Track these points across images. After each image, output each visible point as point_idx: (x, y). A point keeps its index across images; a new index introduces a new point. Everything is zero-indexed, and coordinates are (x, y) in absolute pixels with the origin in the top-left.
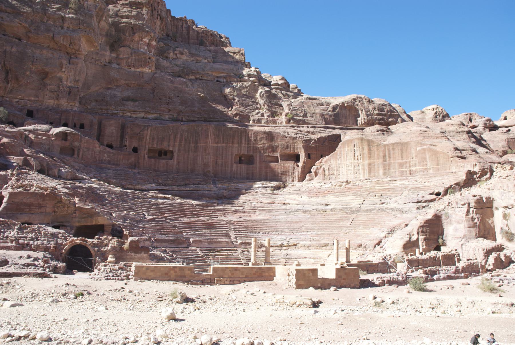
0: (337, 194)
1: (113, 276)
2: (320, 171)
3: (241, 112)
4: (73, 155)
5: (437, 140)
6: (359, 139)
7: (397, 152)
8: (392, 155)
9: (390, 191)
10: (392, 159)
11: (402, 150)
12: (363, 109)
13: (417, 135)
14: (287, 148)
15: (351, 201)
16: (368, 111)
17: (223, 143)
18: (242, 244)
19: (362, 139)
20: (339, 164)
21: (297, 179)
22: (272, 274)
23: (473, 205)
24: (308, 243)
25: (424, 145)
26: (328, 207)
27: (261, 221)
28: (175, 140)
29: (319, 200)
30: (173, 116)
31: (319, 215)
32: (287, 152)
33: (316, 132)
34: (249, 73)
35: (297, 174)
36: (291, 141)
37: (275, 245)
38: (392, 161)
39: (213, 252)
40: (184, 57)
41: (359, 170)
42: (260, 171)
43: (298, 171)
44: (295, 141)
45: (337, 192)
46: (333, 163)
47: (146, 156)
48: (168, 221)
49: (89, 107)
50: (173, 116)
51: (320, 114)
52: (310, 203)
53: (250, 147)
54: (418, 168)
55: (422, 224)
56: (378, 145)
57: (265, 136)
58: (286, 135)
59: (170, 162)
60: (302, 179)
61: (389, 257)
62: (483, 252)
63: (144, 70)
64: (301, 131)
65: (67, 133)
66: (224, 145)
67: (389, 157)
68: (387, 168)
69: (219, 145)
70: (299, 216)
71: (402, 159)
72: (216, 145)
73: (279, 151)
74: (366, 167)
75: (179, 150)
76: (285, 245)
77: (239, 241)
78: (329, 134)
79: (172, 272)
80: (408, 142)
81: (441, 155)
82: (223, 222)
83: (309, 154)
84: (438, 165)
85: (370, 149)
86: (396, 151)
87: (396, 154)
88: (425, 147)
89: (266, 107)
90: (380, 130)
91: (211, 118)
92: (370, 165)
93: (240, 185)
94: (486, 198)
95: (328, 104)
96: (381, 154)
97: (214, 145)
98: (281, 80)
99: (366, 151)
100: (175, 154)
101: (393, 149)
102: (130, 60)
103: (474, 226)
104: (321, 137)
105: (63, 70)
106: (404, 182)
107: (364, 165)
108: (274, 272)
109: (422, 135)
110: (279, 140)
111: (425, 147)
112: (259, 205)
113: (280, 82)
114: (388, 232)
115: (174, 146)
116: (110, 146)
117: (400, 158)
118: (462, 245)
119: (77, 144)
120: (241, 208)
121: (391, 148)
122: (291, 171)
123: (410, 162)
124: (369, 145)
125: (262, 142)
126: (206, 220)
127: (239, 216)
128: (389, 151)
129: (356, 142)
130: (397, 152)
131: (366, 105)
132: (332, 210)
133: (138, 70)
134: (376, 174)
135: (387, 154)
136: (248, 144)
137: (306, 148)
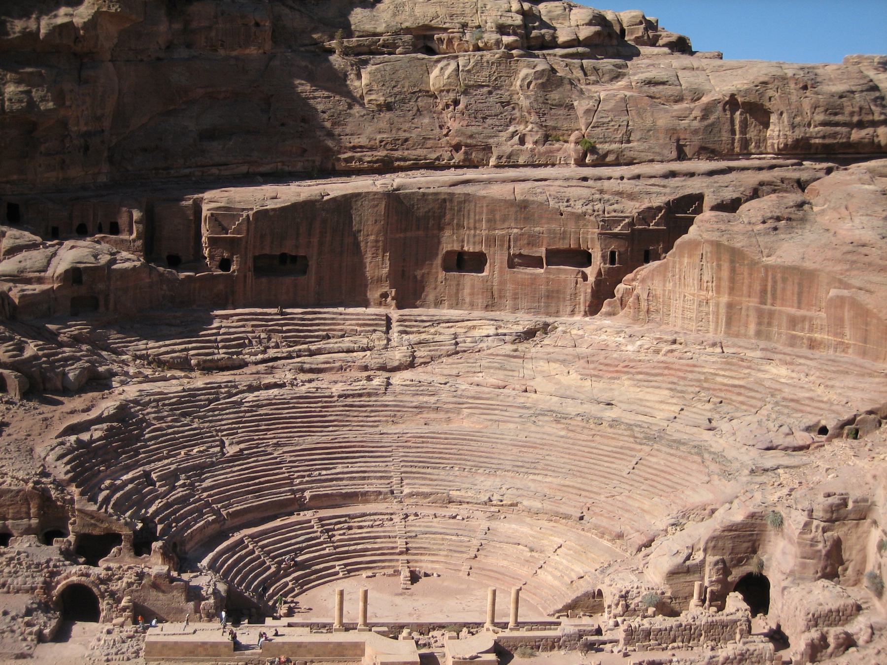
0: (640, 377)
1: (116, 654)
3: (471, 137)
4: (96, 307)
6: (712, 243)
7: (791, 289)
8: (779, 291)
9: (739, 394)
10: (778, 301)
11: (800, 285)
12: (783, 109)
13: (838, 254)
14: (564, 238)
15: (657, 406)
16: (799, 112)
17: (418, 229)
18: (411, 495)
19: (717, 245)
20: (670, 291)
21: (582, 308)
22: (359, 652)
23: (819, 513)
24: (536, 504)
25: (847, 286)
26: (610, 414)
30: (314, 161)
31: (586, 431)
32: (562, 245)
33: (640, 193)
34: (500, 22)
37: (475, 501)
39: (345, 522)
41: (708, 314)
42: (500, 291)
43: (586, 290)
44: (581, 223)
45: (641, 373)
46: (657, 286)
47: (250, 274)
48: (269, 450)
49: (130, 168)
50: (314, 161)
51: (667, 131)
52: (577, 395)
53: (479, 235)
54: (826, 337)
55: (717, 533)
56: (753, 264)
57: (513, 210)
58: (562, 206)
60: (593, 309)
61: (635, 591)
62: (804, 618)
63: (247, 51)
64: (601, 192)
65: (79, 268)
66: (421, 233)
68: (765, 320)
69: (409, 234)
70: (547, 429)
71: (799, 307)
72: (402, 235)
73: (545, 243)
74: (723, 311)
76: (494, 502)
77: (407, 490)
78: (671, 198)
79: (200, 649)
80: (816, 270)
81: (875, 321)
82: (386, 439)
83: (613, 254)
84: (865, 342)
85: (733, 270)
87: (789, 293)
88: (845, 293)
89: (533, 118)
90: (771, 218)
91: (398, 160)
92: (730, 306)
94: (855, 502)
96: (757, 287)
97: (398, 236)
98: (587, 24)
99: (725, 274)
100: (313, 264)
101: (784, 280)
102: (213, 34)
103: (815, 555)
105: (68, 103)
107: (717, 305)
108: (363, 651)
109: (849, 257)
110: (544, 221)
111: (845, 293)
113: (585, 32)
114: (673, 521)
117: (796, 305)
118: (784, 588)
119: (101, 286)
120: (433, 399)
121: (779, 275)
122: (569, 292)
123: (811, 319)
124: (732, 262)
125: (506, 225)
126: (351, 436)
127: (423, 421)
128: (775, 282)
129: (706, 249)
131: (794, 98)
132: (614, 423)
134: (743, 331)
135: (769, 288)
136: (475, 228)
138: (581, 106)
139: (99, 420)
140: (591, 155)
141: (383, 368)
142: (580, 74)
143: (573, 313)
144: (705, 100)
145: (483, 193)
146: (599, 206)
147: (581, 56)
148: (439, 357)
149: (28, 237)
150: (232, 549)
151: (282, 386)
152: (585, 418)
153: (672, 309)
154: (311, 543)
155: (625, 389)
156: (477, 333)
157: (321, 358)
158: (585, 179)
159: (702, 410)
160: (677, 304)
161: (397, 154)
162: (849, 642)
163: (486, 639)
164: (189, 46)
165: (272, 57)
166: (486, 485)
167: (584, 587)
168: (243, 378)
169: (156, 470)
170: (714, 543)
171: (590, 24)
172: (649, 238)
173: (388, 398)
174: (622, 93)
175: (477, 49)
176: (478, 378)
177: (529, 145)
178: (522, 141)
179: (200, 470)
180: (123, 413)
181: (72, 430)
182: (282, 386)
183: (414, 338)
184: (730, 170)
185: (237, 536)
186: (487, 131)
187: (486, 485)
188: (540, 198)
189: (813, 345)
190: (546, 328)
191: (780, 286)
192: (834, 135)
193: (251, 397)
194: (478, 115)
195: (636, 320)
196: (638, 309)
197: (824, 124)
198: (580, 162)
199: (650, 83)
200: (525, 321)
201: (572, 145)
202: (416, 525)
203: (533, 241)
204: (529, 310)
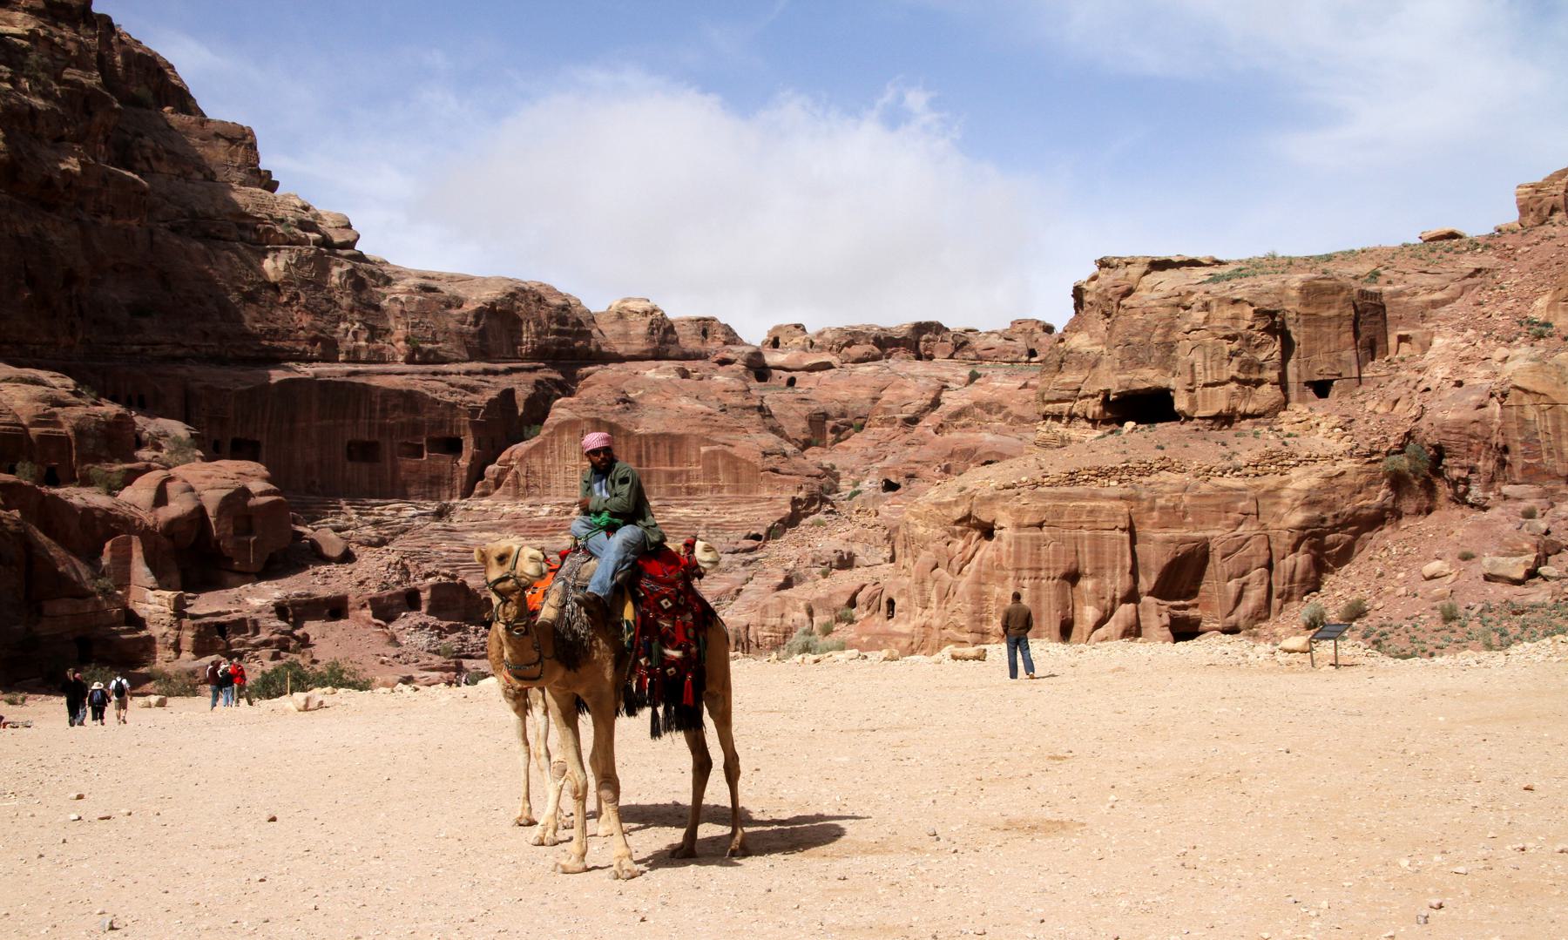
2: (509, 477)
5: (733, 436)
7: (663, 450)
11: (671, 447)
35: (458, 482)
36: (448, 413)
38: (653, 467)
46: (535, 462)
56: (629, 435)
58: (436, 396)
60: (467, 493)
64: (452, 385)
67: (648, 459)
71: (672, 465)
86: (661, 449)
87: (661, 455)
93: (387, 513)
95: (459, 302)
100: (264, 449)
101: (656, 445)
102: (103, 198)
104: (491, 400)
106: (685, 510)
112: (455, 556)
128: (648, 447)
130: (663, 450)
133: (119, 223)
137: (475, 426)
143: (451, 497)
148: (396, 534)
153: (553, 482)
156: (403, 514)
158: (435, 373)
160: (558, 478)
161: (276, 344)
189: (690, 491)
191: (652, 450)
192: (560, 344)
195: (517, 496)
196: (517, 485)
197: (557, 332)
201: (402, 344)
204: (417, 496)
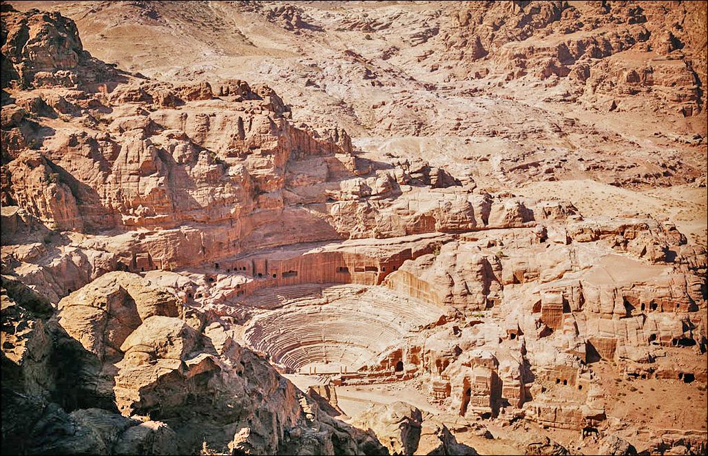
26: (378, 318)
27: (341, 325)
28: (298, 265)
29: (376, 311)
40: (305, 183)
59: (296, 277)
60: (379, 283)
68: (419, 293)
75: (301, 270)
89: (363, 223)
92: (411, 288)
96: (417, 284)
100: (299, 273)
113: (380, 190)
115: (297, 268)
116: (260, 275)
126: (311, 325)
131: (442, 215)
138: (377, 219)
139: (252, 328)
140: (380, 236)
141: (319, 304)
142: (378, 206)
144: (416, 215)
145: (346, 251)
146: (380, 254)
147: (378, 199)
149: (224, 276)
150: (285, 358)
151: (293, 312)
152: (371, 319)
154: (303, 355)
155: (383, 312)
157: (302, 302)
159: (399, 319)
162: (413, 377)
163: (340, 376)
164: (259, 208)
165: (284, 209)
166: (345, 338)
167: (365, 364)
168: (283, 310)
169: (267, 339)
170: (391, 355)
171: (382, 187)
172: (392, 265)
173: (321, 314)
174: (389, 214)
175: (346, 200)
176: (345, 307)
177: (362, 232)
178: (359, 230)
179: (276, 338)
180: (256, 325)
181: (247, 331)
182: (293, 312)
183: (328, 294)
184: (422, 239)
185: (285, 355)
186: (349, 228)
187: (345, 338)
188: (363, 253)
190: (365, 290)
192: (454, 226)
193: (285, 316)
194: (346, 223)
198: (376, 238)
199: (399, 209)
200: (360, 287)
202: (328, 349)
203: (362, 264)
